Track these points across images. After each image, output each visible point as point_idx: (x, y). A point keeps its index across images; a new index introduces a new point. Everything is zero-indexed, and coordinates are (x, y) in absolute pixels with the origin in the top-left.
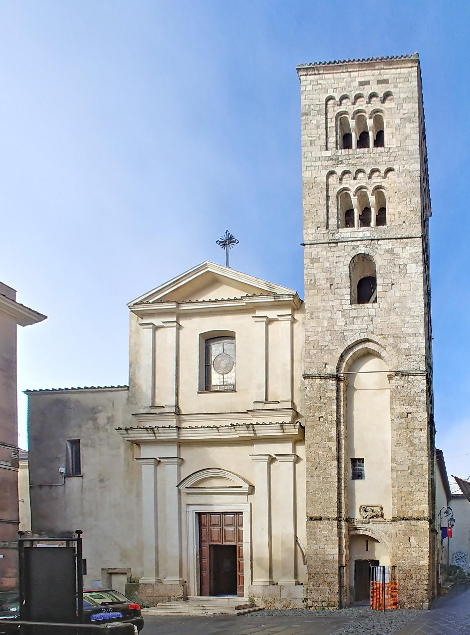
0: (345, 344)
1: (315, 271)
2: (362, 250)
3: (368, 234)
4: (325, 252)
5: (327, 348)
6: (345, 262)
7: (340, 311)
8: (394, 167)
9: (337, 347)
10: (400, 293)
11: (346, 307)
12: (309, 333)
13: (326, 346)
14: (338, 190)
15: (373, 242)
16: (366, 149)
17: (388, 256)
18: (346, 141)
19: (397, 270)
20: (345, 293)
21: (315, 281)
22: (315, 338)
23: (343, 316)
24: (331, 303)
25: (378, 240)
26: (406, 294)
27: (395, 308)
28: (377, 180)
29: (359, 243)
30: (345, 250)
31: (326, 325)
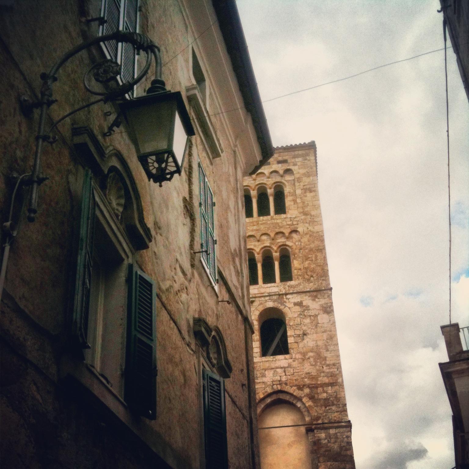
2: (270, 304)
10: (312, 343)
15: (281, 296)
17: (297, 308)
19: (307, 321)
25: (286, 294)
27: (309, 358)
28: (281, 240)
29: (267, 298)
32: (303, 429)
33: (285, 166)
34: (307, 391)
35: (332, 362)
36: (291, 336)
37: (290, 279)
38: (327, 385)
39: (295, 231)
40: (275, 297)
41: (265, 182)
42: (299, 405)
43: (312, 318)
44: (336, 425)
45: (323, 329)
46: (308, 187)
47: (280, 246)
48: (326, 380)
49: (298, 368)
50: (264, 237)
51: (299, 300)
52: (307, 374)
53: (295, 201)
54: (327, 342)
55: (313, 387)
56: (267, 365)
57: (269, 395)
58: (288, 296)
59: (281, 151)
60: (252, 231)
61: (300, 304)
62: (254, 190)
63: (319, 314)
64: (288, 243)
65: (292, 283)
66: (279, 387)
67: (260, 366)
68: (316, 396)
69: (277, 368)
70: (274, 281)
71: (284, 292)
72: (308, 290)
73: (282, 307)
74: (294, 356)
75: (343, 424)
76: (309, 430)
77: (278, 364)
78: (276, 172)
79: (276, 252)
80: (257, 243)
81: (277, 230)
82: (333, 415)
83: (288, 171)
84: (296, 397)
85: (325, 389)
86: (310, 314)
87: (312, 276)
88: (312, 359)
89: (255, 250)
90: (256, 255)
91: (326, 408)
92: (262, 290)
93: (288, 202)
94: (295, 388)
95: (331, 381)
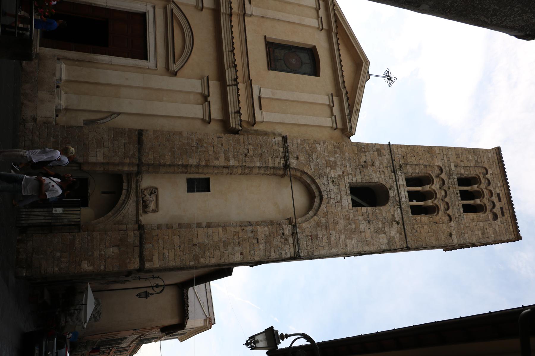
0: (316, 177)
1: (371, 152)
2: (392, 194)
3: (404, 199)
4: (386, 161)
5: (311, 159)
6: (380, 179)
7: (343, 173)
8: (452, 222)
9: (313, 169)
10: (363, 228)
11: (346, 178)
12: (322, 144)
13: (313, 159)
14: (432, 174)
15: (399, 204)
16: (460, 198)
18: (462, 181)
19: (380, 225)
20: (357, 179)
21: (363, 152)
22: (319, 149)
23: (339, 176)
24: (348, 165)
25: (401, 208)
26: (363, 234)
27: (350, 224)
28: (442, 206)
29: (396, 191)
30: (390, 178)
31: (330, 159)
32: (291, 215)
33: (499, 214)
34: (323, 220)
35: (348, 244)
36: (367, 209)
37: (413, 213)
38: (329, 239)
39: (450, 220)
40: (397, 198)
41: (486, 197)
42: (311, 213)
43: (383, 229)
44: (296, 244)
45: (374, 238)
46: (486, 231)
47: (437, 206)
48: (333, 238)
50: (443, 193)
52: (337, 221)
53: (473, 221)
54: (364, 241)
55: (326, 227)
56: (343, 188)
57: (318, 188)
58: (399, 210)
59: (511, 211)
60: (448, 183)
62: (478, 187)
63: (387, 235)
65: (410, 214)
67: (341, 181)
68: (320, 228)
69: (341, 197)
70: (462, 199)
71: (402, 206)
72: (406, 227)
73: (389, 203)
74: (351, 211)
75: (297, 250)
76: (290, 221)
77: (344, 197)
78: (494, 206)
79: (432, 202)
80: (438, 186)
81: (450, 204)
82: (304, 242)
83: (495, 217)
84: (317, 211)
85: (326, 236)
86: (386, 228)
87: (416, 231)
88: (349, 226)
89: (432, 185)
90: (428, 186)
91: (310, 236)
92: (402, 188)
93: (472, 215)
94: (325, 210)
95: (332, 242)
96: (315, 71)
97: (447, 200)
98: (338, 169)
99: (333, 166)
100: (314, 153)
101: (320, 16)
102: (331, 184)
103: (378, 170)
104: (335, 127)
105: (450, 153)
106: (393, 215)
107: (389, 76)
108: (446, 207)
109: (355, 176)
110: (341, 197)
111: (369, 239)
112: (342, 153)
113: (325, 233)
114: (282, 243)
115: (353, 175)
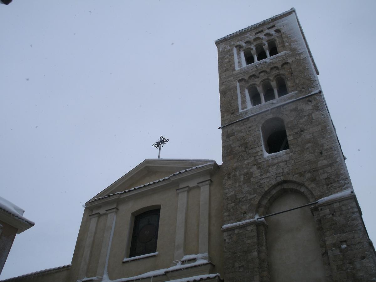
0: (263, 191)
1: (231, 142)
4: (238, 128)
5: (244, 199)
7: (254, 165)
8: (288, 61)
9: (254, 196)
12: (227, 191)
13: (243, 197)
22: (232, 193)
23: (258, 168)
24: (246, 162)
26: (315, 134)
27: (308, 148)
28: (275, 72)
30: (255, 121)
31: (242, 179)
34: (308, 175)
36: (289, 135)
38: (327, 166)
39: (286, 63)
42: (303, 189)
47: (275, 77)
49: (299, 158)
50: (262, 74)
51: (294, 107)
52: (307, 161)
54: (323, 132)
55: (314, 171)
57: (274, 187)
58: (284, 107)
61: (295, 110)
63: (312, 112)
64: (281, 72)
66: (282, 178)
68: (317, 178)
69: (280, 162)
74: (294, 150)
79: (273, 81)
80: (257, 79)
85: (325, 170)
88: (310, 149)
89: (256, 85)
91: (328, 186)
94: (297, 176)
95: (330, 162)
96: (155, 211)
97: (268, 70)
98: (251, 170)
99: (248, 176)
100: (238, 197)
101: (105, 212)
102: (268, 174)
103: (248, 133)
104: (209, 182)
105: (225, 76)
106: (291, 111)
107: (160, 143)
108: (276, 69)
109: (257, 152)
110: (280, 162)
111: (320, 127)
112: (236, 169)
113: (321, 171)
114: (341, 214)
115: (256, 155)
